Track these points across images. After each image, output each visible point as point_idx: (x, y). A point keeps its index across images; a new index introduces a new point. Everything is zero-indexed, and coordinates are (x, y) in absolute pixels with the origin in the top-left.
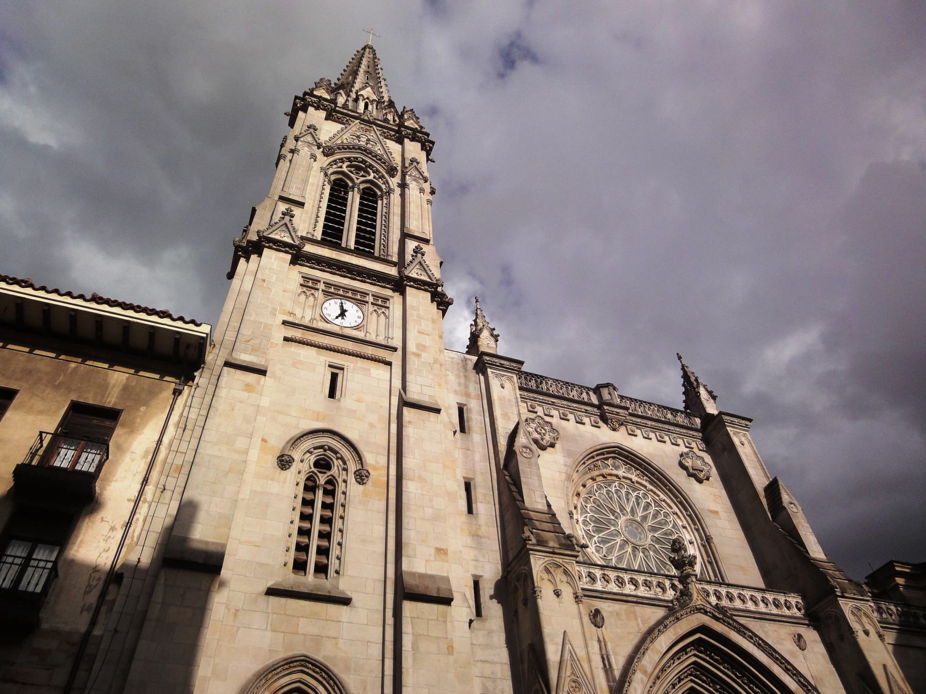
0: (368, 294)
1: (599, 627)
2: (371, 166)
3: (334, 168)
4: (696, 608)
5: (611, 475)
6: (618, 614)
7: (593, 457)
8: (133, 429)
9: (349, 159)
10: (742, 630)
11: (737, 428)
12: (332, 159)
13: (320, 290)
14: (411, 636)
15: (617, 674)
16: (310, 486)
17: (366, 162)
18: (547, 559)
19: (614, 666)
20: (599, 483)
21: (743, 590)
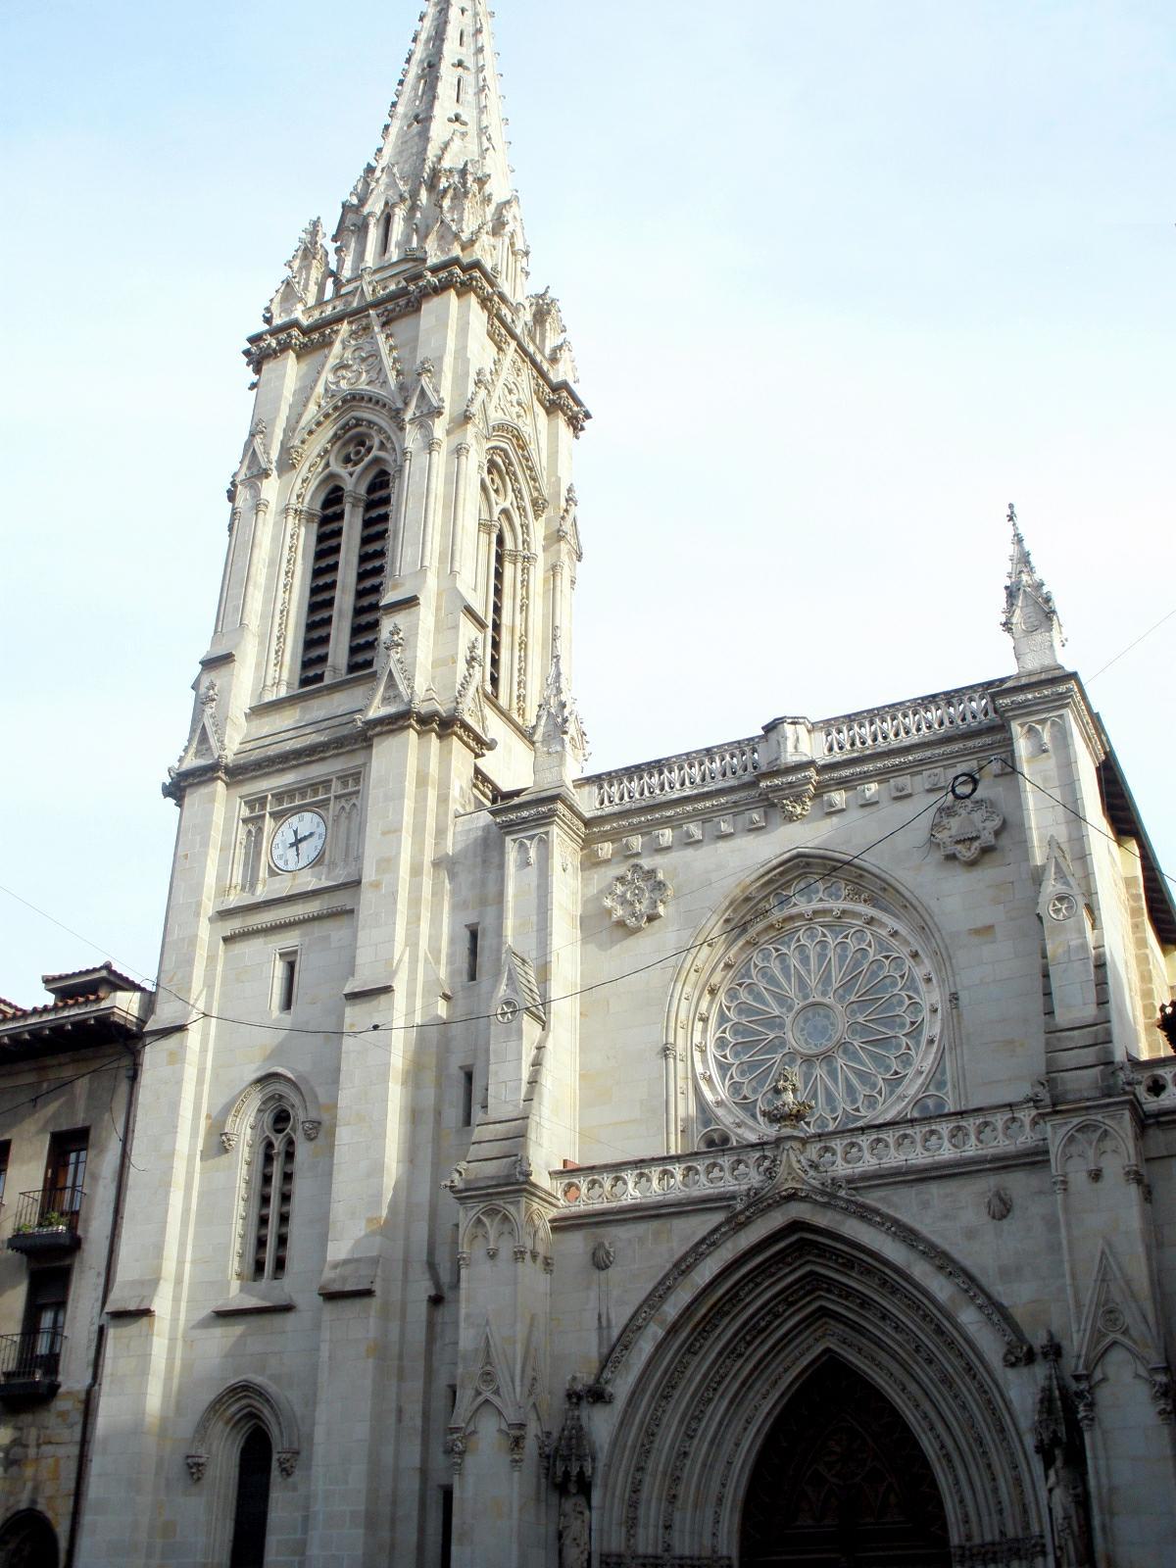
0: (331, 780)
2: (370, 423)
5: (791, 918)
6: (641, 1240)
8: (102, 1151)
10: (865, 1214)
13: (268, 815)
15: (615, 1333)
18: (482, 1205)
19: (614, 1322)
20: (764, 946)
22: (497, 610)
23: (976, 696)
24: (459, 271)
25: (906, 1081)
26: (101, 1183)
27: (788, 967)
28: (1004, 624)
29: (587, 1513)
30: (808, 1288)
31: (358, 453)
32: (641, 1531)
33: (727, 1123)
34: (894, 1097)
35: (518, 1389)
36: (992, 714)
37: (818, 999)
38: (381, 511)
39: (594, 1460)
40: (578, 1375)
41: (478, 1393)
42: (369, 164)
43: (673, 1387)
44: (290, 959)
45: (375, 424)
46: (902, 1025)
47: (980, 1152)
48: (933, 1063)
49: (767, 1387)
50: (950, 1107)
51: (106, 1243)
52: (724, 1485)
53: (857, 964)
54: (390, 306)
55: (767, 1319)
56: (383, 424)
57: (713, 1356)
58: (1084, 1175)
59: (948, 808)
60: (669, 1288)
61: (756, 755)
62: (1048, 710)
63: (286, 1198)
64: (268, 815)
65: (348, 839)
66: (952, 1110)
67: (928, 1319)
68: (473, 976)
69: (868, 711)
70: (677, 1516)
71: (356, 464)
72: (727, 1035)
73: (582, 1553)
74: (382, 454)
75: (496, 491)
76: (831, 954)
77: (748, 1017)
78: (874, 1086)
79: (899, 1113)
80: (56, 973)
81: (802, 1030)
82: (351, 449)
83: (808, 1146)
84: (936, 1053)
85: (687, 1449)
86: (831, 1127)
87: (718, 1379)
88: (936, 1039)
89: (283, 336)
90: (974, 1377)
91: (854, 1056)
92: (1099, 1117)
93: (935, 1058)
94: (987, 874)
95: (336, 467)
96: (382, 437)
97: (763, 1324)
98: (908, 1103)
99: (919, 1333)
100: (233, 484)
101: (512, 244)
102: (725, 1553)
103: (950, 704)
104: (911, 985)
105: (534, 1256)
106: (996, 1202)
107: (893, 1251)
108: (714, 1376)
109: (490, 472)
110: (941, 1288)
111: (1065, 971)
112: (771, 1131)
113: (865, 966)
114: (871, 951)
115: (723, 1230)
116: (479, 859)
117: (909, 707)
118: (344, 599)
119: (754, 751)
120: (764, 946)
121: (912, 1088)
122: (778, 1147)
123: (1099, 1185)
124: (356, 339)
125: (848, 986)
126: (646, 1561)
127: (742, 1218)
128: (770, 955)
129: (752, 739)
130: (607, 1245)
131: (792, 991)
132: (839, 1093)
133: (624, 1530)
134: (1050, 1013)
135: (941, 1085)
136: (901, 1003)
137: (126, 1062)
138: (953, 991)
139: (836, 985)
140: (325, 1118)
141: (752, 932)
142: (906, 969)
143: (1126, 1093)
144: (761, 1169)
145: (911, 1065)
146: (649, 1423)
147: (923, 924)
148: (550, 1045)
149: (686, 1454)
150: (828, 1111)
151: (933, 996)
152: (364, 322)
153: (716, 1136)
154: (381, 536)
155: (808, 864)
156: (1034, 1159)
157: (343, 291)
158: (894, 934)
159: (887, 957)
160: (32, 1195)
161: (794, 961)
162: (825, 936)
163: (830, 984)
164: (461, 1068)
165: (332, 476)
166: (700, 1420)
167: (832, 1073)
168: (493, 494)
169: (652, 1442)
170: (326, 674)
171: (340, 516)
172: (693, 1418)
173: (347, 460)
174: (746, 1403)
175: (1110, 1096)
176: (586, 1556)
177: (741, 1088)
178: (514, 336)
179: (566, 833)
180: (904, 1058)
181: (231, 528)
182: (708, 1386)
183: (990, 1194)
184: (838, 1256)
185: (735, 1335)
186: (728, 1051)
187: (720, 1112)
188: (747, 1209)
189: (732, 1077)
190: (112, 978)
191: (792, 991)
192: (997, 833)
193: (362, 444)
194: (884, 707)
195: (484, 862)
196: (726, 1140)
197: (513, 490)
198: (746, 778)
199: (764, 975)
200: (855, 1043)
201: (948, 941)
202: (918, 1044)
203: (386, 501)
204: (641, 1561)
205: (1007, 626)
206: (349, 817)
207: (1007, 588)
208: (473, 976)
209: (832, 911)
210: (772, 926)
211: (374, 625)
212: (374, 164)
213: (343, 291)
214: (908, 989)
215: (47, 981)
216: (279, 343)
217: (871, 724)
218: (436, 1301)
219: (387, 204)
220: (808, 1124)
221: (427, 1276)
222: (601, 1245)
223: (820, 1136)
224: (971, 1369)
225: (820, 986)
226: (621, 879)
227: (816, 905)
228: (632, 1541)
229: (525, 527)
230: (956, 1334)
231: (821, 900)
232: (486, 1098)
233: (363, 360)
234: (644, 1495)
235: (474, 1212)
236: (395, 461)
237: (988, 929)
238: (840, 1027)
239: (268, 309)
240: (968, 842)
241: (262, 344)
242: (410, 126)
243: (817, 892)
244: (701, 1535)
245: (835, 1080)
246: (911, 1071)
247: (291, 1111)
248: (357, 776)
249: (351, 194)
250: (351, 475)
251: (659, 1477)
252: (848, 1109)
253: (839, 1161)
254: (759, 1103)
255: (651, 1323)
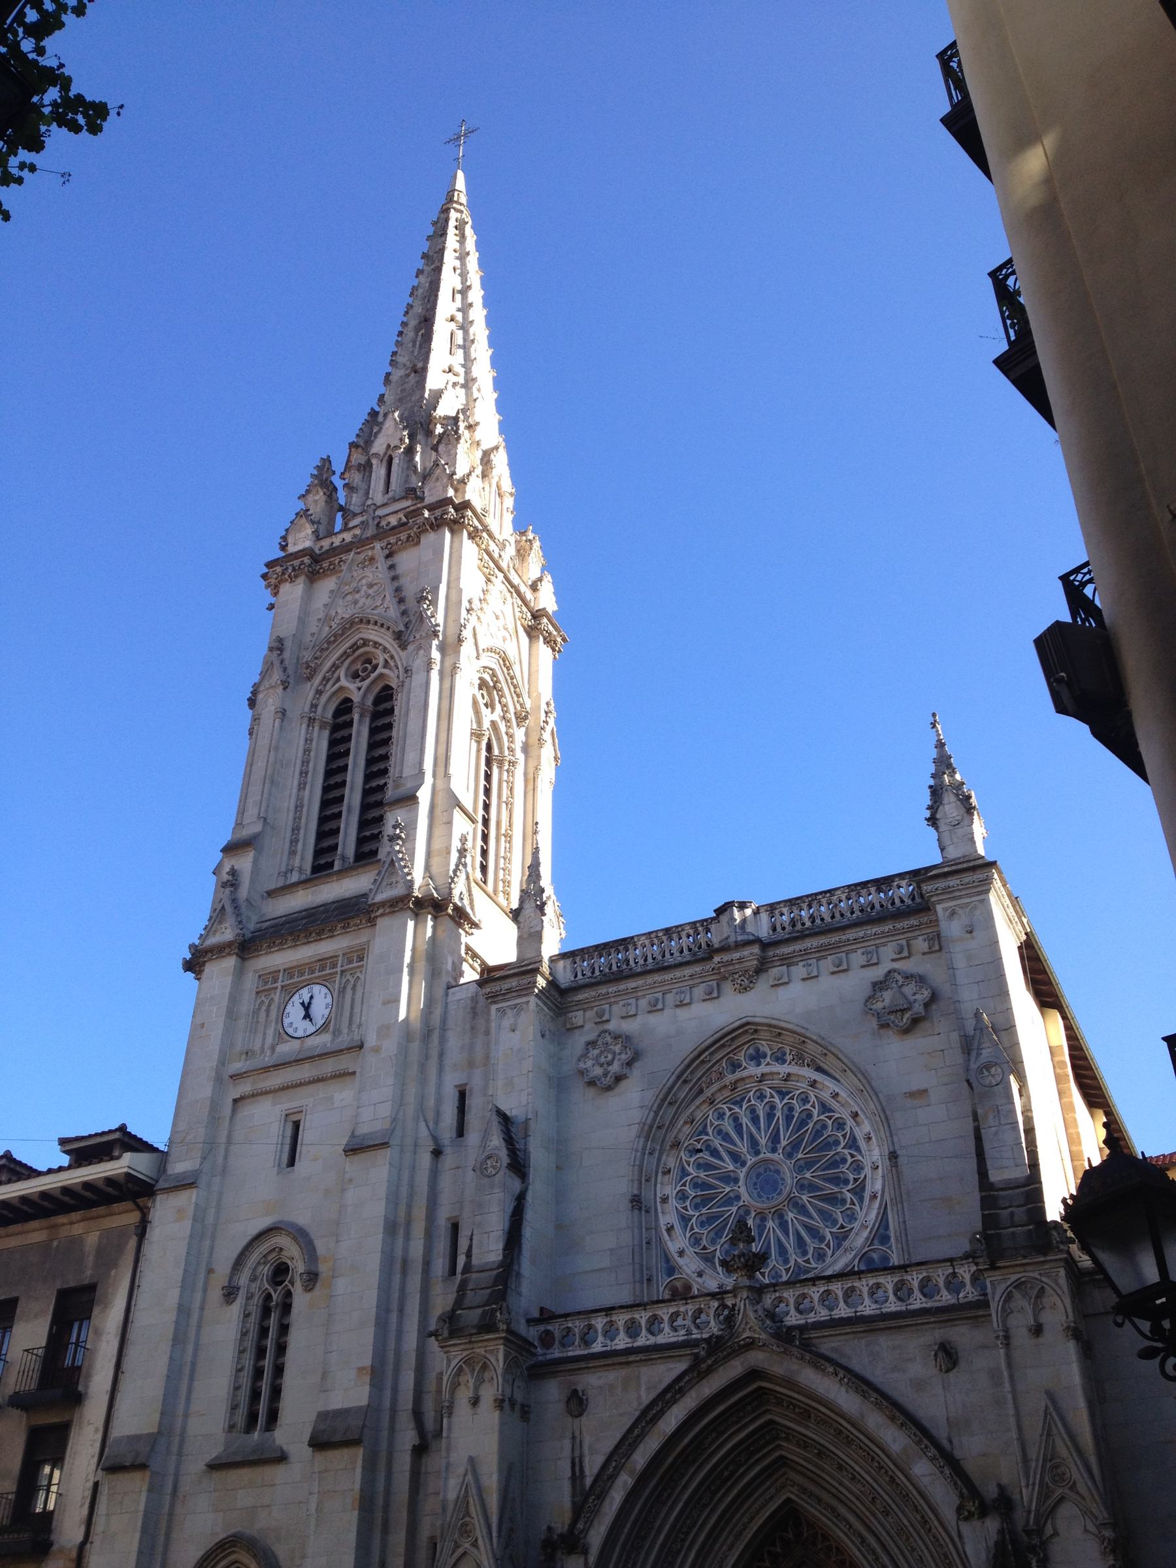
1: (576, 1417)
2: (376, 645)
3: (330, 689)
4: (739, 1346)
7: (703, 1062)
8: (106, 1305)
9: (345, 655)
11: (960, 897)
12: (317, 680)
14: (316, 1496)
15: (588, 1481)
16: (266, 1311)
17: (370, 641)
18: (465, 1353)
19: (587, 1471)
20: (719, 1106)
21: (860, 1279)
22: (487, 807)
23: (904, 883)
24: (452, 511)
25: (852, 1234)
26: (105, 1338)
27: (741, 1125)
28: (928, 820)
30: (768, 1437)
31: (365, 670)
33: (689, 1272)
34: (842, 1249)
36: (918, 900)
37: (769, 1155)
38: (386, 720)
40: (553, 1525)
41: (457, 1546)
42: (372, 409)
44: (295, 1118)
45: (380, 645)
46: (846, 1182)
47: (924, 1305)
48: (877, 1217)
49: (731, 1538)
50: (895, 1260)
51: (106, 1398)
53: (803, 1123)
54: (392, 540)
55: (731, 1468)
56: (388, 646)
57: (681, 1505)
58: (1024, 1332)
59: (881, 983)
60: (638, 1436)
61: (709, 935)
62: (967, 896)
63: (281, 1349)
64: (279, 988)
65: (352, 1008)
66: (896, 1264)
67: (883, 1471)
68: (461, 1132)
69: (807, 896)
71: (363, 680)
72: (687, 1188)
74: (386, 671)
75: (486, 705)
76: (779, 1114)
77: (705, 1171)
78: (822, 1239)
79: (847, 1265)
80: (73, 1135)
81: (755, 1184)
82: (358, 666)
83: (764, 1296)
84: (879, 1208)
86: (785, 1278)
87: (685, 1530)
88: (879, 1195)
89: (296, 563)
90: (930, 1530)
91: (802, 1210)
92: (1036, 1275)
93: (878, 1213)
94: (918, 1043)
95: (344, 682)
96: (386, 656)
97: (726, 1474)
98: (855, 1257)
99: (875, 1485)
100: (255, 693)
101: (498, 487)
103: (879, 890)
104: (853, 1144)
105: (512, 1403)
106: (940, 1354)
107: (846, 1400)
109: (480, 688)
110: (894, 1439)
111: (996, 1133)
112: (729, 1282)
113: (811, 1125)
114: (815, 1112)
115: (687, 1378)
116: (468, 1026)
117: (843, 893)
118: (353, 796)
119: (708, 930)
120: (719, 1106)
121: (859, 1239)
122: (735, 1296)
123: (1041, 1340)
124: (363, 568)
125: (795, 1146)
127: (704, 1366)
128: (724, 1114)
129: (706, 920)
130: (581, 1394)
131: (743, 1147)
132: (790, 1245)
134: (982, 1172)
135: (885, 1239)
136: (844, 1161)
137: (134, 1217)
138: (891, 1150)
139: (784, 1143)
140: (323, 1268)
141: (708, 1093)
142: (848, 1129)
143: (1061, 1251)
144: (721, 1318)
145: (856, 1219)
147: (862, 1087)
148: (529, 1197)
150: (781, 1262)
151: (874, 1154)
152: (370, 553)
153: (678, 1284)
154: (387, 741)
155: (756, 1031)
156: (976, 1311)
157: (351, 524)
158: (835, 1096)
159: (830, 1118)
160: (35, 1352)
161: (745, 1121)
162: (773, 1097)
163: (779, 1142)
164: (448, 1219)
165: (341, 688)
167: (783, 1225)
168: (483, 708)
170: (336, 863)
171: (350, 724)
173: (355, 676)
175: (1045, 1255)
177: (701, 1239)
178: (500, 569)
179: (545, 1004)
180: (849, 1212)
181: (251, 734)
183: (936, 1347)
184: (795, 1406)
185: (701, 1484)
186: (688, 1203)
187: (681, 1261)
188: (709, 1355)
189: (692, 1229)
190: (126, 1139)
191: (743, 1147)
192: (927, 1005)
193: (369, 661)
194: (821, 893)
195: (473, 1028)
196: (688, 1287)
197: (500, 702)
198: (700, 955)
199: (720, 1132)
200: (803, 1197)
201: (884, 1104)
202: (861, 1199)
203: (391, 711)
205: (933, 821)
206: (354, 988)
207: (931, 787)
208: (461, 1132)
209: (779, 1073)
210: (725, 1086)
211: (380, 819)
212: (377, 409)
213: (351, 524)
214: (850, 1148)
215: (63, 1142)
216: (294, 570)
217: (810, 907)
218: (421, 1450)
219: (389, 446)
220: (763, 1274)
221: (412, 1425)
222: (575, 1392)
223: (774, 1286)
224: (926, 1522)
225: (769, 1143)
226: (592, 1044)
227: (763, 1069)
229: (511, 736)
230: (911, 1488)
231: (768, 1064)
232: (470, 1246)
233: (370, 586)
235: (456, 1361)
236: (398, 677)
237: (923, 1093)
238: (789, 1181)
239: (284, 538)
240: (899, 1014)
241: (279, 569)
242: (408, 375)
243: (765, 1056)
245: (786, 1233)
246: (857, 1225)
247: (289, 1262)
248: (360, 954)
249: (358, 436)
250: (359, 689)
252: (800, 1260)
253: (793, 1311)
254: (718, 1253)
255: (622, 1473)
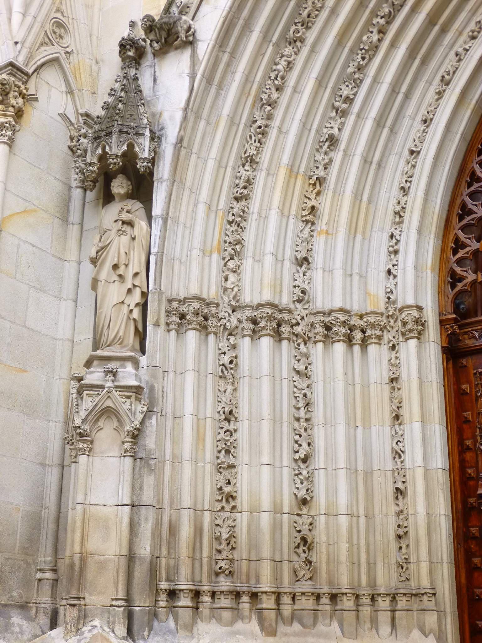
29: (141, 224)
32: (248, 264)
35: (16, 18)
39: (156, 138)
43: (307, 25)
52: (404, 190)
70: (319, 242)
73: (129, 291)
85: (335, 131)
87: (386, 9)
102: (410, 301)
108: (378, 6)
126: (258, 314)
133: (215, 257)
146: (262, 84)
149: (333, 141)
166: (358, 83)
169: (270, 117)
172: (343, 79)
174: (440, 51)
176: (137, 297)
182: (369, 22)
204: (249, 313)
228: (232, 278)
234: (255, 205)
244: (363, 277)
251: (282, 173)
